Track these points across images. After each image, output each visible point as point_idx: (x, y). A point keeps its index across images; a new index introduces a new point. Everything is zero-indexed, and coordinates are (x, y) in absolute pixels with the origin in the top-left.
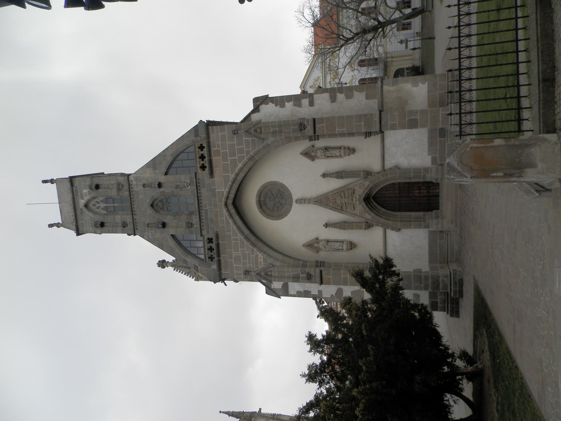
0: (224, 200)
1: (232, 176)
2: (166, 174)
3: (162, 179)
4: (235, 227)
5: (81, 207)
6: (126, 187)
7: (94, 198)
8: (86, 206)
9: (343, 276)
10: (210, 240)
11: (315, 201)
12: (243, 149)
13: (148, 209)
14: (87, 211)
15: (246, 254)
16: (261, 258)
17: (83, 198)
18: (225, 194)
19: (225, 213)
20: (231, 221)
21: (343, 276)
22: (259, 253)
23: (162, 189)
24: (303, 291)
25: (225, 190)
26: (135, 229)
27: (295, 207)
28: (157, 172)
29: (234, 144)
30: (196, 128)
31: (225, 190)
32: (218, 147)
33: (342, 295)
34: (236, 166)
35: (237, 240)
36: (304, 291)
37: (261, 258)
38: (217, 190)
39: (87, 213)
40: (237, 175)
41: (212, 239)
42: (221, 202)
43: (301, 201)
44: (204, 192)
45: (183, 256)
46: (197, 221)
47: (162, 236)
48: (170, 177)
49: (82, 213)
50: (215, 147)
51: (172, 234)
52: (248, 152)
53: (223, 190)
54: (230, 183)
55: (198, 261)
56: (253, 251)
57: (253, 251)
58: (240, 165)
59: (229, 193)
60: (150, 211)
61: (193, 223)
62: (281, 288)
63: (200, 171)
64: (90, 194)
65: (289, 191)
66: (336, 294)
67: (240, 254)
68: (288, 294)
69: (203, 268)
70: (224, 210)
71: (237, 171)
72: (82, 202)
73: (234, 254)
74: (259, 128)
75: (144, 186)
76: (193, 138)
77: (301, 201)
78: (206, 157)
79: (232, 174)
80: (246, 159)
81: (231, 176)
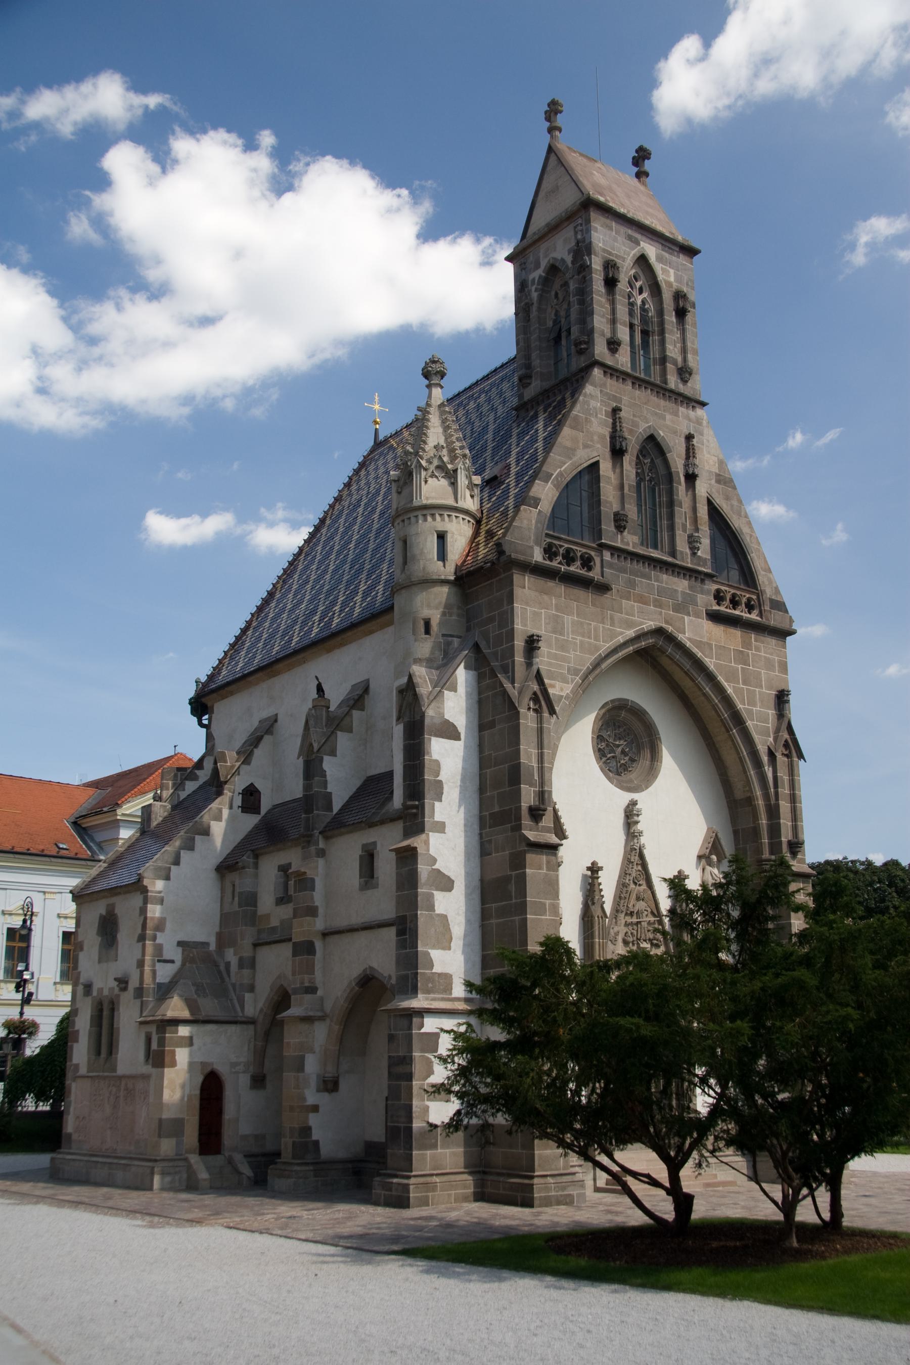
0: (670, 629)
1: (710, 663)
2: (710, 503)
3: (702, 488)
4: (621, 639)
5: (641, 243)
6: (681, 388)
7: (655, 288)
8: (642, 260)
9: (548, 902)
10: (587, 563)
11: (640, 849)
12: (755, 706)
13: (647, 425)
14: (634, 255)
15: (569, 653)
16: (562, 690)
17: (660, 259)
18: (680, 637)
19: (646, 623)
20: (631, 633)
21: (548, 902)
22: (571, 686)
23: (682, 479)
24: (438, 778)
25: (689, 639)
26: (607, 370)
27: (625, 797)
28: (713, 482)
29: (761, 687)
30: (780, 606)
31: (689, 639)
32: (758, 649)
33: (437, 889)
34: (727, 681)
35: (597, 638)
36: (441, 782)
37: (562, 690)
38: (686, 617)
39: (633, 252)
40: (711, 677)
41: (590, 569)
42: (667, 622)
43: (631, 815)
44: (681, 585)
45: (556, 478)
46: (628, 544)
47: (595, 438)
48: (703, 511)
49: (630, 238)
50: (756, 641)
51: (602, 466)
52: (750, 712)
53: (687, 635)
54: (700, 655)
55: (548, 515)
56: (576, 672)
57: (576, 672)
58: (730, 691)
59: (680, 646)
60: (642, 428)
61: (625, 533)
62: (446, 717)
63: (715, 587)
64: (669, 284)
65: (647, 788)
66: (438, 871)
67: (568, 634)
68: (431, 735)
69: (534, 522)
70: (652, 623)
71: (720, 678)
72: (651, 250)
73: (568, 620)
74: (790, 752)
75: (689, 438)
76: (768, 596)
77: (631, 815)
78: (748, 615)
79: (715, 665)
80: (740, 706)
81: (711, 662)
